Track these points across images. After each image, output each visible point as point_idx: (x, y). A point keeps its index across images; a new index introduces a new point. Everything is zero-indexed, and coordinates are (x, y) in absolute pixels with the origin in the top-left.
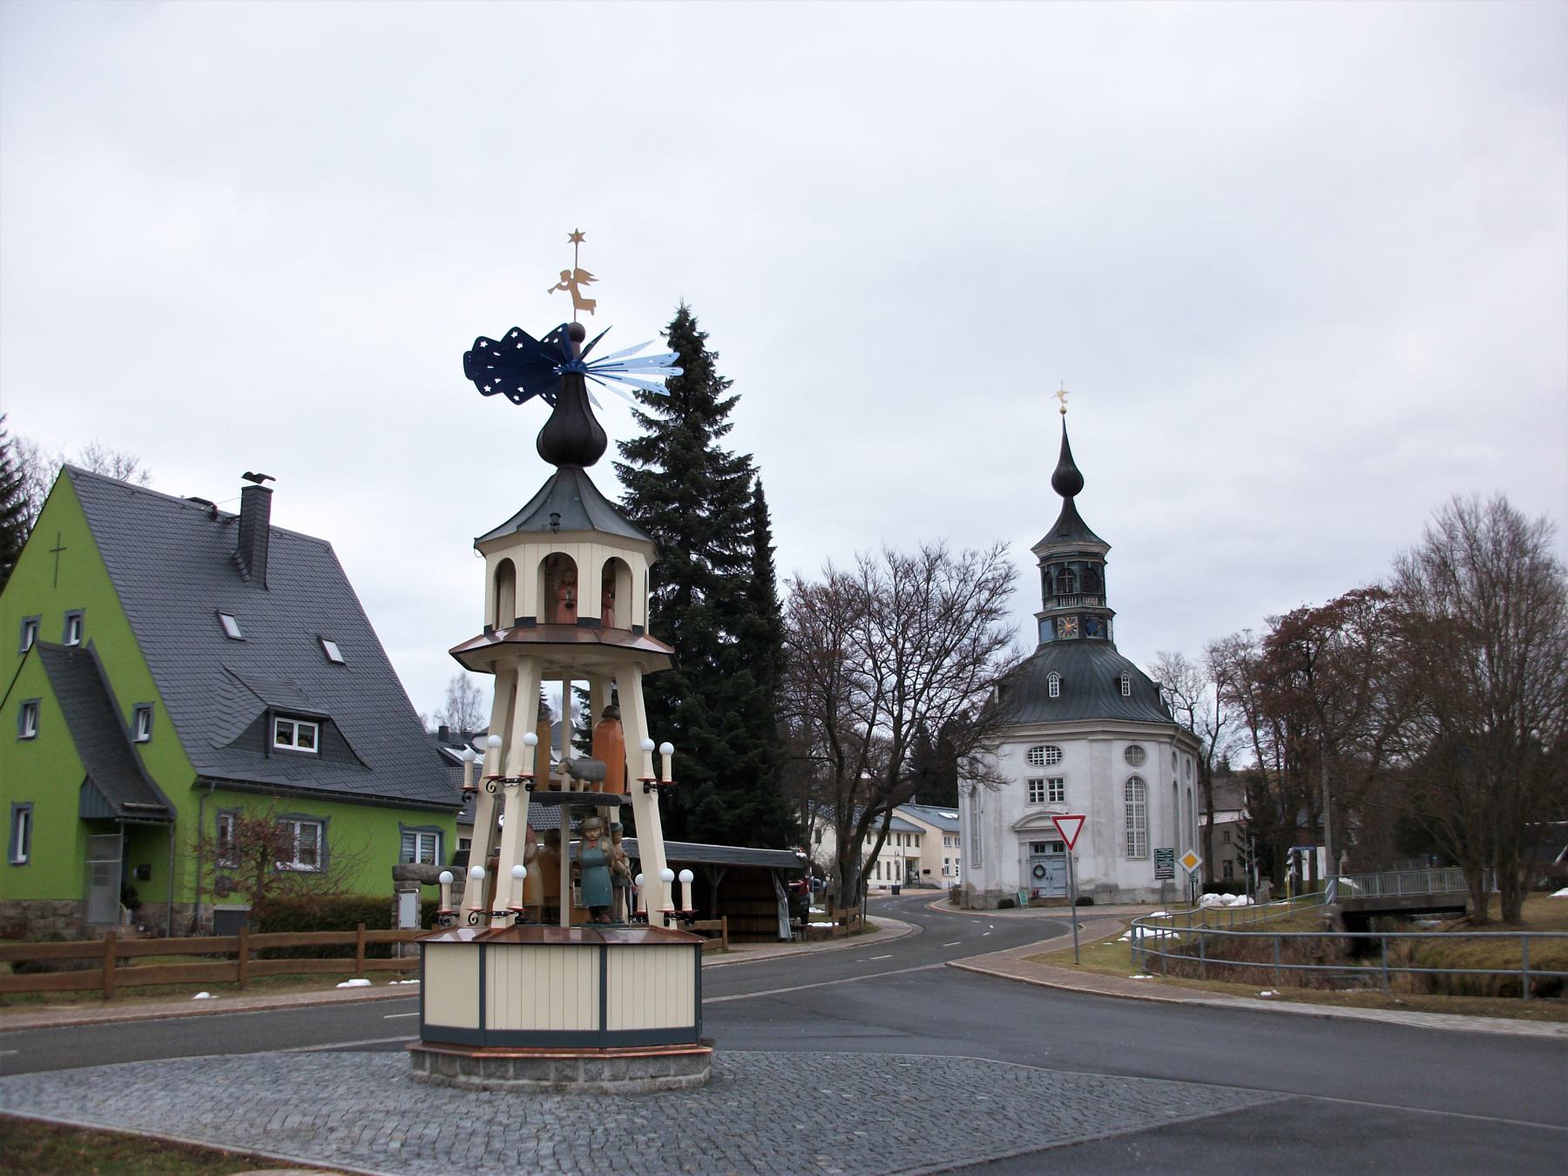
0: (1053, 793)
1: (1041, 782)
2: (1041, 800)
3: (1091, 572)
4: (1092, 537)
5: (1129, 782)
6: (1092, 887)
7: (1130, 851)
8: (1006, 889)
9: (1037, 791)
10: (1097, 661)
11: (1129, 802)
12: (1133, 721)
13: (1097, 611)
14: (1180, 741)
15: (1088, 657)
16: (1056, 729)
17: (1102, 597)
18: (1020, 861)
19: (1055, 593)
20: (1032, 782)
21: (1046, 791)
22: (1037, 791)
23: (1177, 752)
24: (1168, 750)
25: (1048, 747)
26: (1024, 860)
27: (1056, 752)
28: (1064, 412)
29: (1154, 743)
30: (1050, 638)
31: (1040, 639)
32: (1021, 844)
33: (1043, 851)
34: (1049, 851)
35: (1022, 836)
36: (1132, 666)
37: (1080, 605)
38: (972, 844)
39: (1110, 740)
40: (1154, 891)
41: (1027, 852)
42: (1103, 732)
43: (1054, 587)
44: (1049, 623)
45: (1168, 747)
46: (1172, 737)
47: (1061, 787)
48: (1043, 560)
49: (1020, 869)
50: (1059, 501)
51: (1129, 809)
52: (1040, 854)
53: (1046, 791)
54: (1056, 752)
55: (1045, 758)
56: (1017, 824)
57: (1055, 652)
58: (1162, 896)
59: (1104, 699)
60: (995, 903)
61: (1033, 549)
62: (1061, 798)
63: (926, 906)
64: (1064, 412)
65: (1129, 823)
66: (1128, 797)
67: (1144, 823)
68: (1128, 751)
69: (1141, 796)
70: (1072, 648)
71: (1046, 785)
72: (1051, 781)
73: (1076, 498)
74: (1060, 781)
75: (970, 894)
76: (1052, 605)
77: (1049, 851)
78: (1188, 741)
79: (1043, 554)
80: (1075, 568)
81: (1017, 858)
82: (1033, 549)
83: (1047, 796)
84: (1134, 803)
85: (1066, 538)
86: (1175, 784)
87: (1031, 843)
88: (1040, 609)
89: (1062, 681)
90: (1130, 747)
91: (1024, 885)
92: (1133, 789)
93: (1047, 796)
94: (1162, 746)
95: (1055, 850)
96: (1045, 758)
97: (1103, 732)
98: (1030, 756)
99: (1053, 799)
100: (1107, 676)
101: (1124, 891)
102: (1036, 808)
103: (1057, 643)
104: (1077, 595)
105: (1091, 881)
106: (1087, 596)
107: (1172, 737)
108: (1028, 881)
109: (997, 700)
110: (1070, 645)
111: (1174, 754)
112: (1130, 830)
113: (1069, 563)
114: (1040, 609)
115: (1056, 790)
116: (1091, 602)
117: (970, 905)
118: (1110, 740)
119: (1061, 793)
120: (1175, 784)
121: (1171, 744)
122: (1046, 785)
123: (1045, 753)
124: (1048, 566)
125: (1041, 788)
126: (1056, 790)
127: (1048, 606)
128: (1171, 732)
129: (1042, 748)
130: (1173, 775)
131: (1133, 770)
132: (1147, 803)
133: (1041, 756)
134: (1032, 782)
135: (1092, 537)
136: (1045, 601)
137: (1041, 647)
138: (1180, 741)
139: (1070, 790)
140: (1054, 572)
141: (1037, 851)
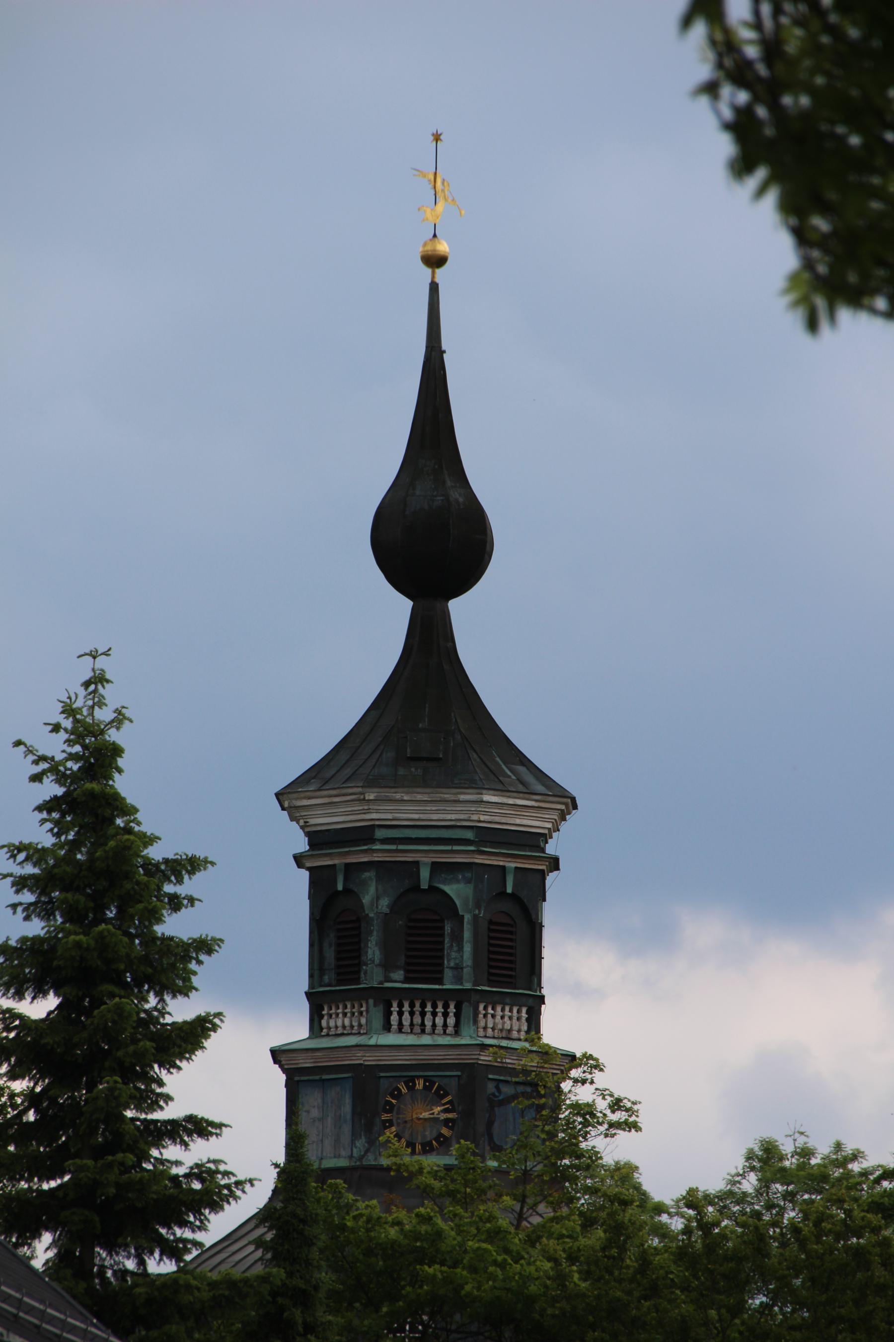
19: (373, 977)
43: (373, 952)
106: (494, 1000)
113: (436, 867)
127: (336, 1020)
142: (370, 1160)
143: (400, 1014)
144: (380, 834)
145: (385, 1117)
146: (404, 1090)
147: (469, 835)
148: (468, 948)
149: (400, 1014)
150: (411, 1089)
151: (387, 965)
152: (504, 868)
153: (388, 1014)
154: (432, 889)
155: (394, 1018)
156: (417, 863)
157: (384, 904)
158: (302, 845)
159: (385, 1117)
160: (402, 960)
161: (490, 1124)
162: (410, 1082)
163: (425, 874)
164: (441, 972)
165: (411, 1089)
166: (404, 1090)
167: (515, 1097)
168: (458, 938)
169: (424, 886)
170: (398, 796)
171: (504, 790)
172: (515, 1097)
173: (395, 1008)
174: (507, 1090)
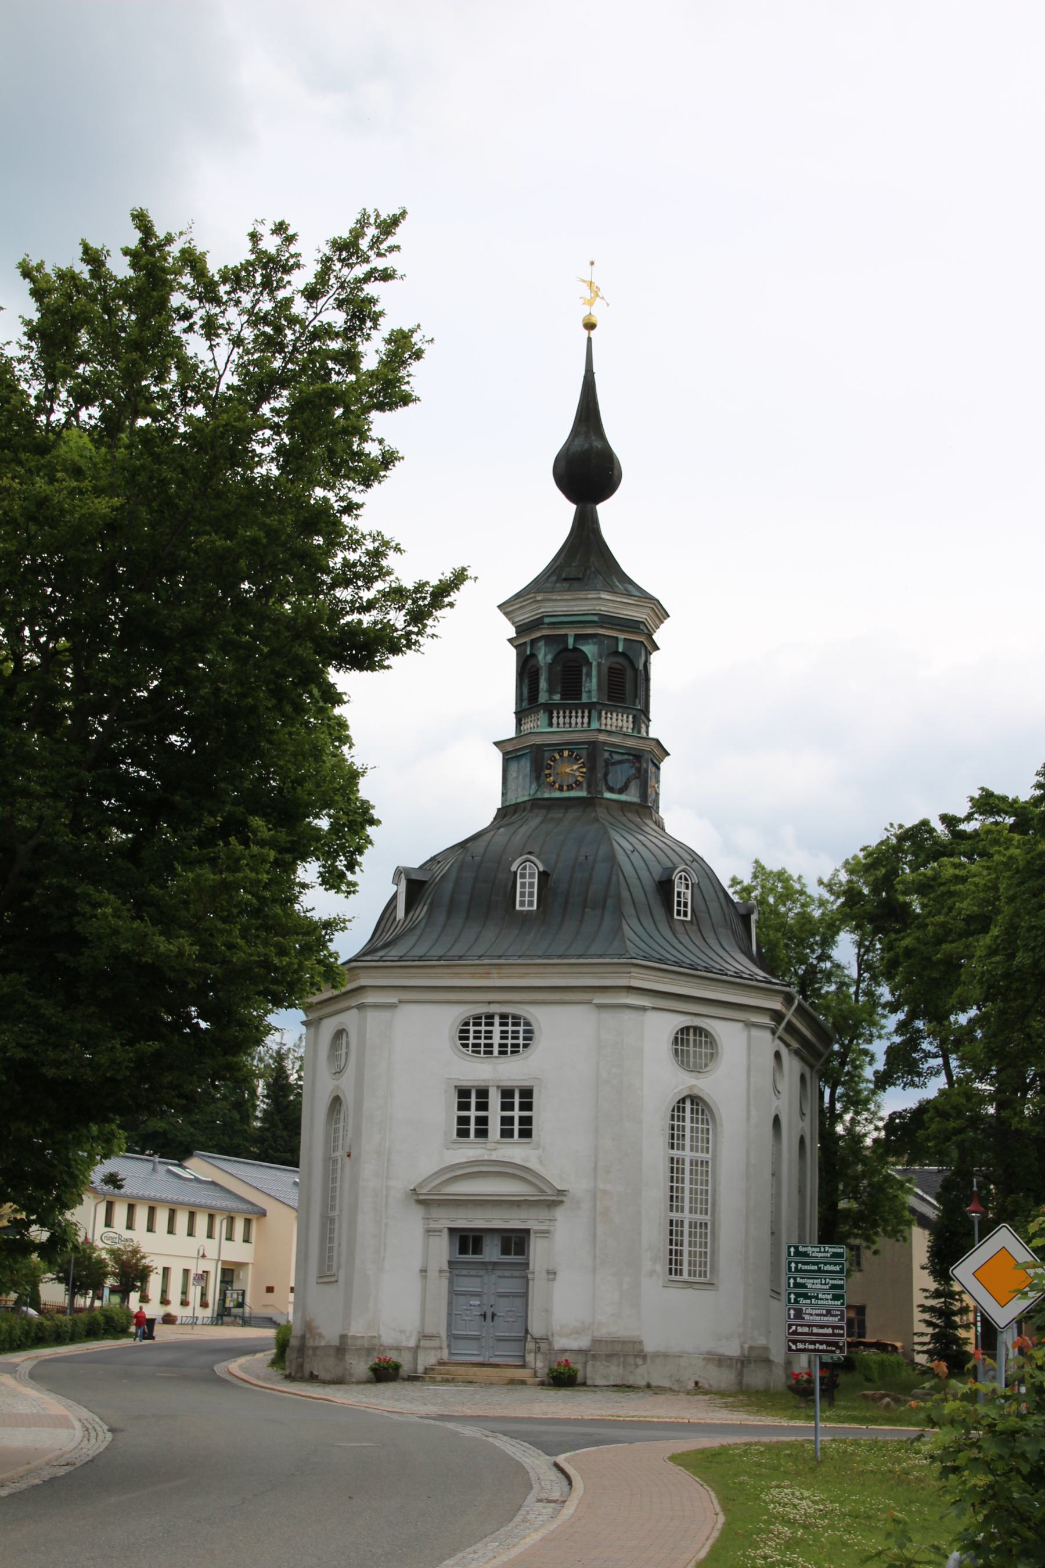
0: (507, 1121)
1: (483, 1093)
2: (482, 1133)
3: (621, 660)
4: (630, 587)
5: (679, 1107)
6: (584, 1343)
7: (674, 1265)
8: (388, 1338)
9: (473, 1113)
10: (623, 842)
11: (675, 1153)
12: (693, 971)
13: (630, 743)
14: (790, 1028)
15: (606, 832)
16: (525, 975)
17: (642, 715)
18: (424, 1271)
19: (543, 698)
20: (463, 1093)
21: (495, 1114)
22: (473, 1113)
23: (784, 1052)
24: (766, 1043)
25: (504, 1016)
26: (433, 1273)
27: (521, 1029)
28: (590, 326)
29: (740, 1025)
30: (522, 795)
31: (504, 795)
32: (429, 1232)
33: (477, 1249)
34: (491, 1251)
35: (436, 1212)
36: (696, 859)
37: (595, 725)
38: (323, 1226)
39: (644, 1009)
40: (721, 1361)
41: (442, 1249)
42: (630, 989)
43: (543, 685)
44: (526, 765)
45: (767, 1035)
46: (777, 1016)
47: (527, 1106)
48: (521, 630)
49: (424, 1290)
50: (566, 511)
51: (675, 1167)
52: (470, 1257)
53: (495, 1114)
54: (521, 1029)
55: (496, 1040)
56: (421, 1185)
57: (534, 822)
58: (741, 1374)
59: (634, 923)
60: (361, 1367)
61: (499, 607)
62: (526, 1133)
63: (219, 1369)
64: (590, 326)
65: (674, 1199)
66: (675, 1139)
67: (706, 1202)
68: (682, 1037)
69: (705, 1140)
70: (572, 814)
71: (495, 1100)
72: (507, 1093)
73: (603, 509)
74: (527, 1093)
75: (310, 1343)
76: (537, 723)
77: (491, 1251)
78: (807, 1033)
79: (526, 616)
80: (589, 649)
81: (417, 1264)
82: (499, 607)
83: (495, 1127)
84: (687, 1154)
85: (576, 584)
86: (777, 1121)
87: (451, 1230)
88: (509, 731)
89: (544, 876)
90: (685, 1030)
91: (429, 1330)
92: (688, 1124)
93: (495, 1127)
94: (755, 1033)
95: (505, 1251)
96: (496, 1040)
97: (630, 989)
98: (463, 1035)
99: (507, 1133)
100: (644, 874)
101: (656, 1355)
102: (471, 1151)
103: (536, 804)
104: (590, 706)
105: (577, 1332)
107: (777, 1016)
108: (439, 1325)
109: (401, 913)
110: (567, 808)
111: (777, 1055)
112: (675, 1216)
113: (577, 637)
114: (509, 731)
115: (517, 1113)
116: (619, 721)
117: (307, 1369)
118: (644, 1009)
119: (526, 1121)
120: (777, 1121)
121: (773, 1032)
122: (495, 1100)
123: (497, 1029)
124: (533, 642)
125: (483, 1106)
126: (517, 1113)
127: (528, 726)
128: (777, 1005)
129: (490, 1017)
130: (776, 1103)
131: (684, 1082)
132: (714, 1157)
133: (489, 1035)
134: (463, 1093)
135: (630, 587)
136: (521, 715)
137: (505, 813)
138: (790, 1028)
139: (540, 1115)
140: (544, 657)
141: (463, 1250)
142: (539, 795)
143: (558, 717)
144: (547, 620)
145: (547, 772)
146: (558, 757)
147: (595, 618)
148: (594, 680)
149: (558, 717)
150: (561, 756)
151: (551, 691)
152: (617, 638)
153: (551, 718)
154: (575, 649)
155: (555, 720)
156: (566, 635)
157: (549, 658)
158: (512, 633)
159: (547, 772)
160: (559, 689)
161: (606, 775)
162: (561, 752)
163: (571, 641)
164: (581, 694)
165: (561, 756)
166: (558, 757)
167: (620, 762)
168: (589, 675)
169: (570, 646)
170: (554, 597)
171: (614, 593)
172: (620, 762)
173: (555, 714)
174: (617, 757)
